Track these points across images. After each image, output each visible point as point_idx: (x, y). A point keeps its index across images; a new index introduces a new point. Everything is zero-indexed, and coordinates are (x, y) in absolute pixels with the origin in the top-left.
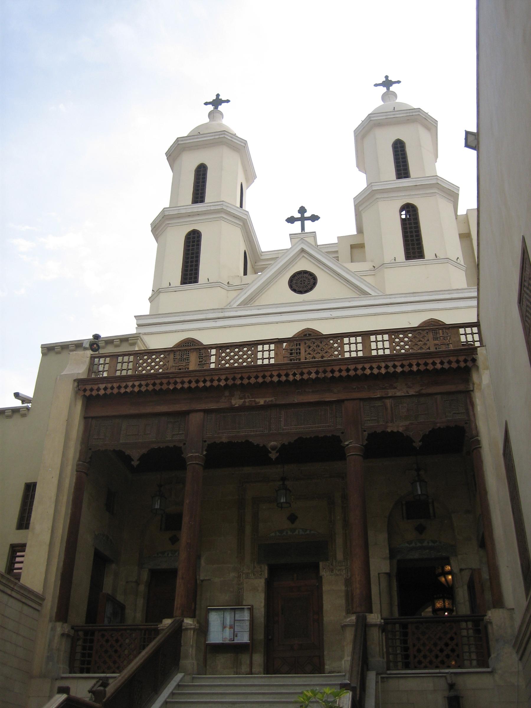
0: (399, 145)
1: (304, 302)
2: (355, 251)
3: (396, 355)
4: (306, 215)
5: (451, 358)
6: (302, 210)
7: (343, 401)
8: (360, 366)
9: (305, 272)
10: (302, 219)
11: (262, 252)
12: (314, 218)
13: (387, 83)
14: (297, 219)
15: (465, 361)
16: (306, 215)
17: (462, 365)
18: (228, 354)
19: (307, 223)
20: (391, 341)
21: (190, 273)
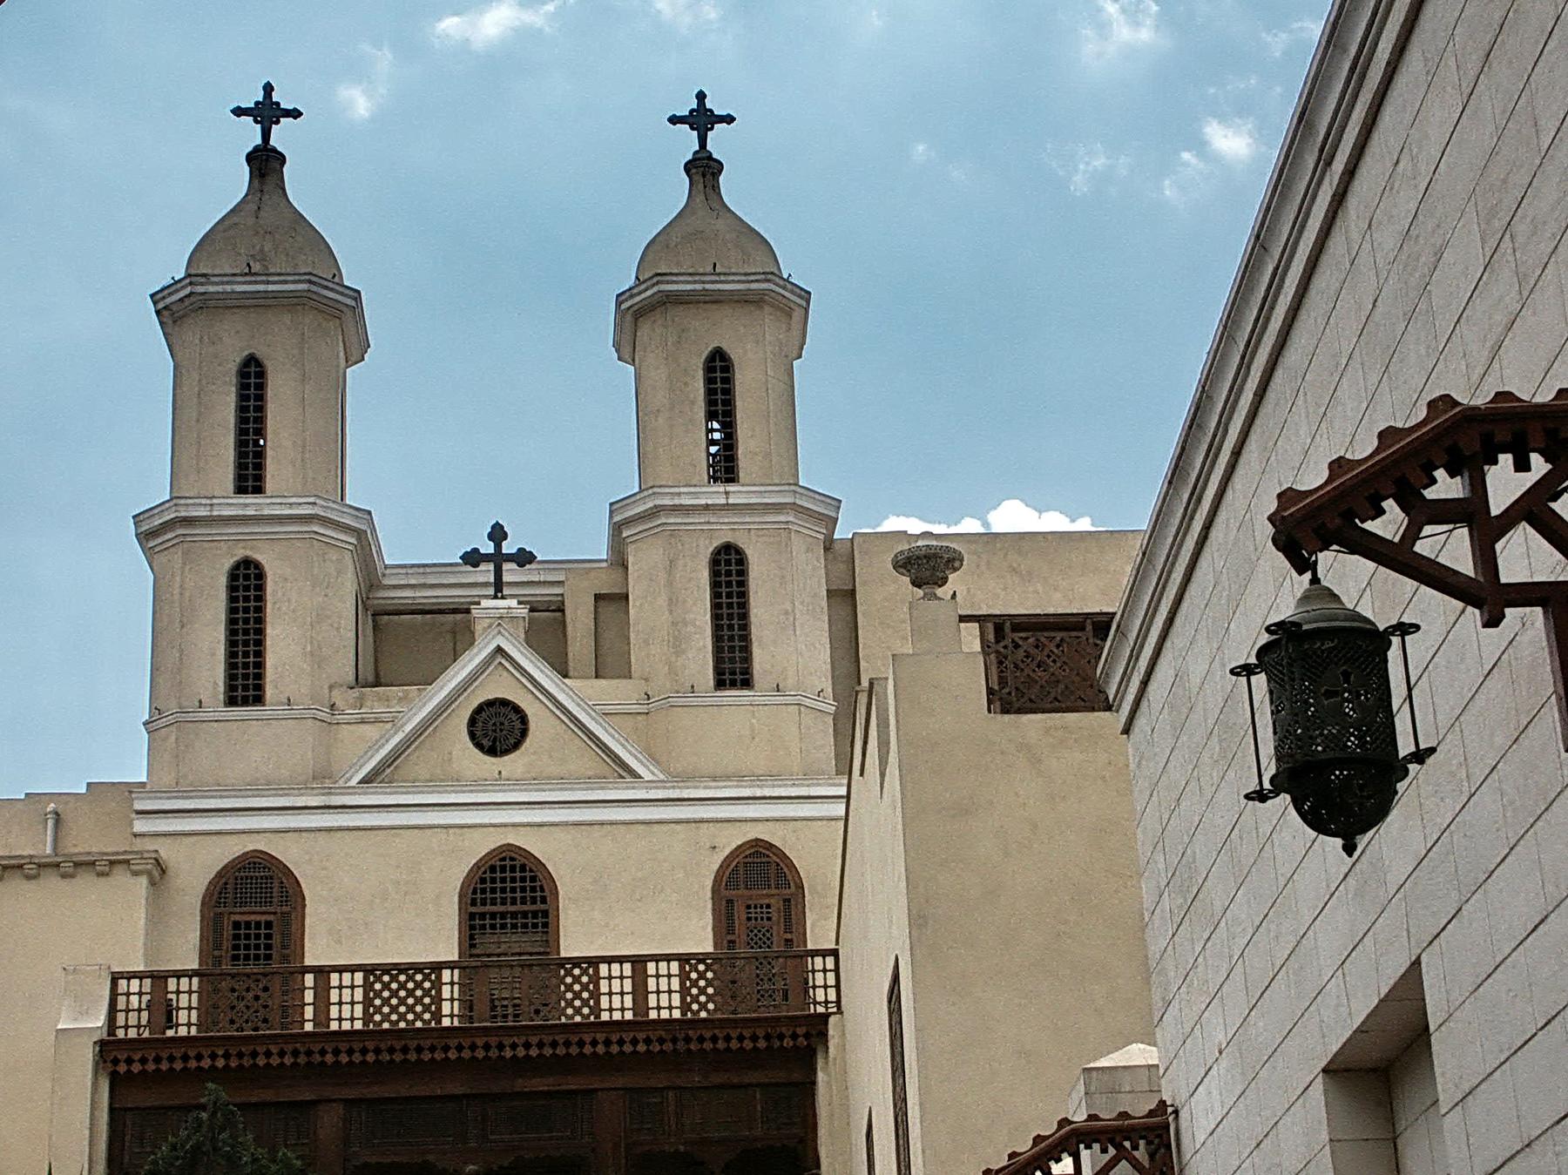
0: (718, 364)
1: (499, 781)
2: (601, 603)
3: (690, 1021)
4: (508, 547)
5: (784, 1030)
6: (498, 534)
7: (596, 1090)
8: (628, 1037)
9: (504, 703)
10: (498, 559)
11: (386, 567)
12: (524, 558)
13: (702, 119)
14: (487, 558)
15: (807, 1036)
16: (508, 547)
17: (802, 1041)
18: (386, 986)
19: (506, 566)
20: (684, 976)
21: (245, 683)
